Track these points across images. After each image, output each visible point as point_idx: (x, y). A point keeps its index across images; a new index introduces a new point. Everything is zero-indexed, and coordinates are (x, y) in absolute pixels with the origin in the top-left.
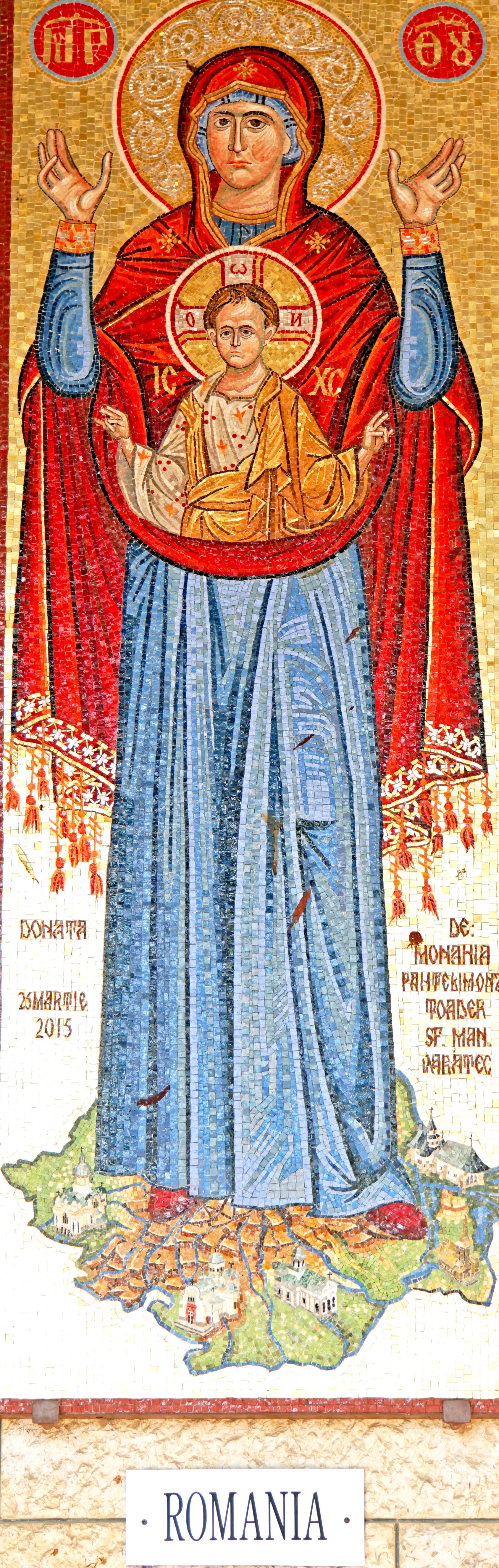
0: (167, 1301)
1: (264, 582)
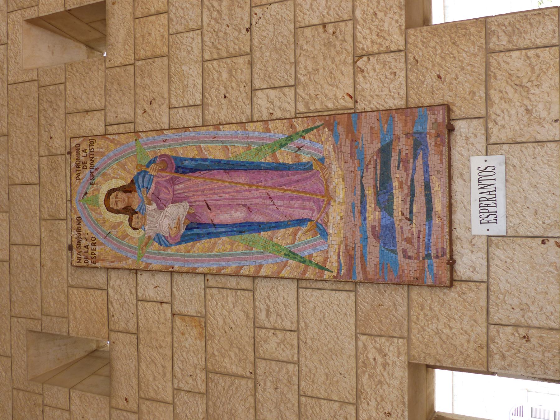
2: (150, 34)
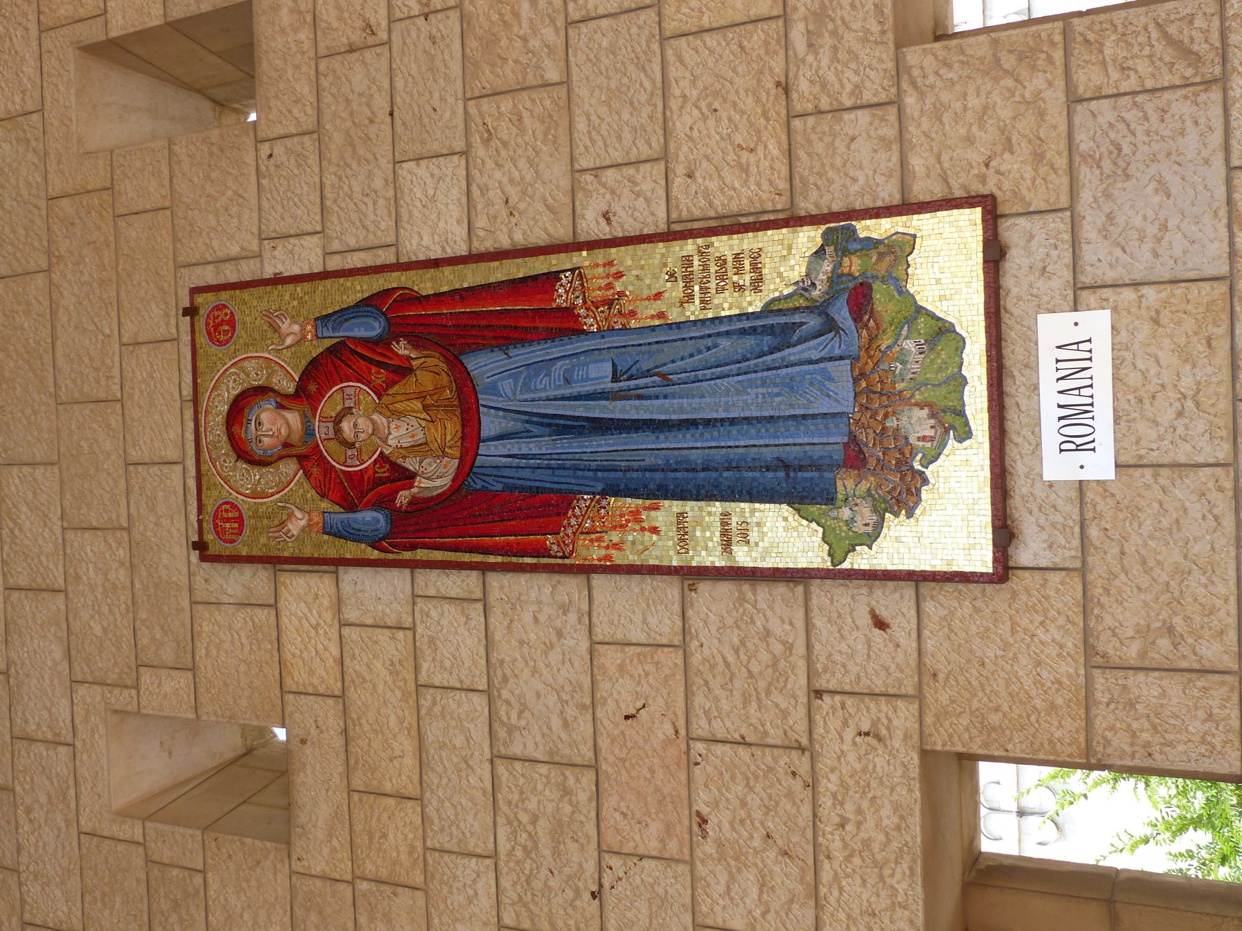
0: (920, 455)
1: (481, 409)
2: (384, 836)
